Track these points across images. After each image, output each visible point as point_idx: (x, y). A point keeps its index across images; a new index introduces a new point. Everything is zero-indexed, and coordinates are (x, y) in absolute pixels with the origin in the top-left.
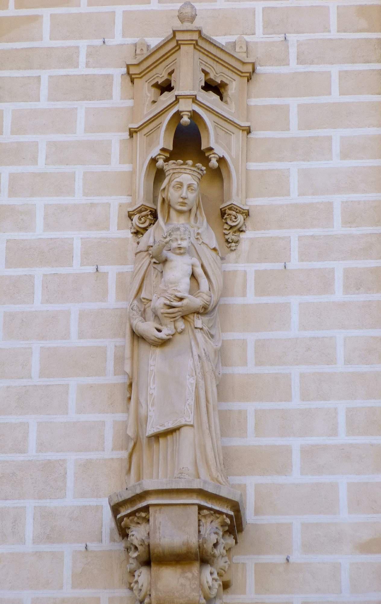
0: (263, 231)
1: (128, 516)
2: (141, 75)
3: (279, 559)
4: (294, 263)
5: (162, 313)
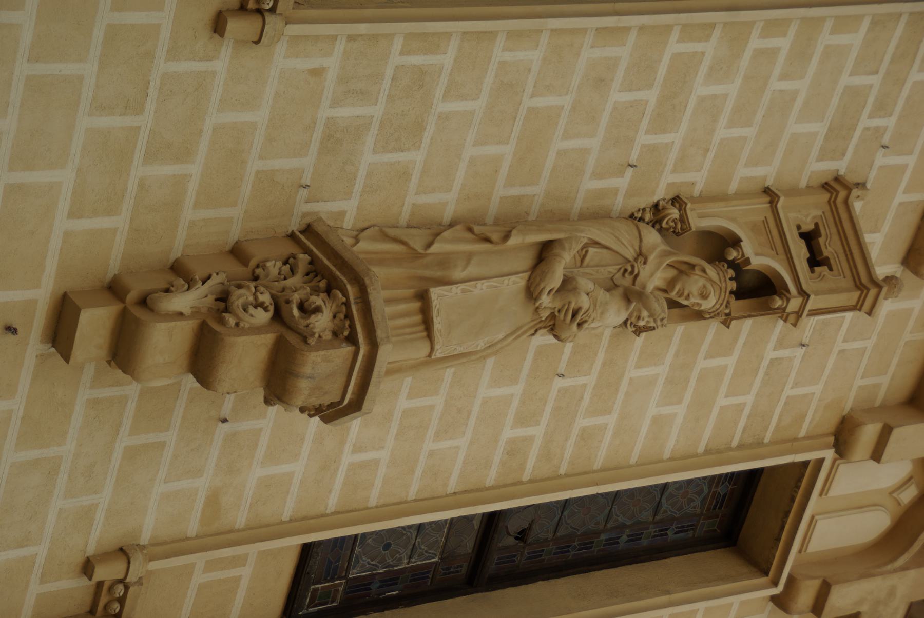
0: (606, 345)
1: (347, 304)
2: (832, 203)
4: (559, 383)
5: (570, 303)
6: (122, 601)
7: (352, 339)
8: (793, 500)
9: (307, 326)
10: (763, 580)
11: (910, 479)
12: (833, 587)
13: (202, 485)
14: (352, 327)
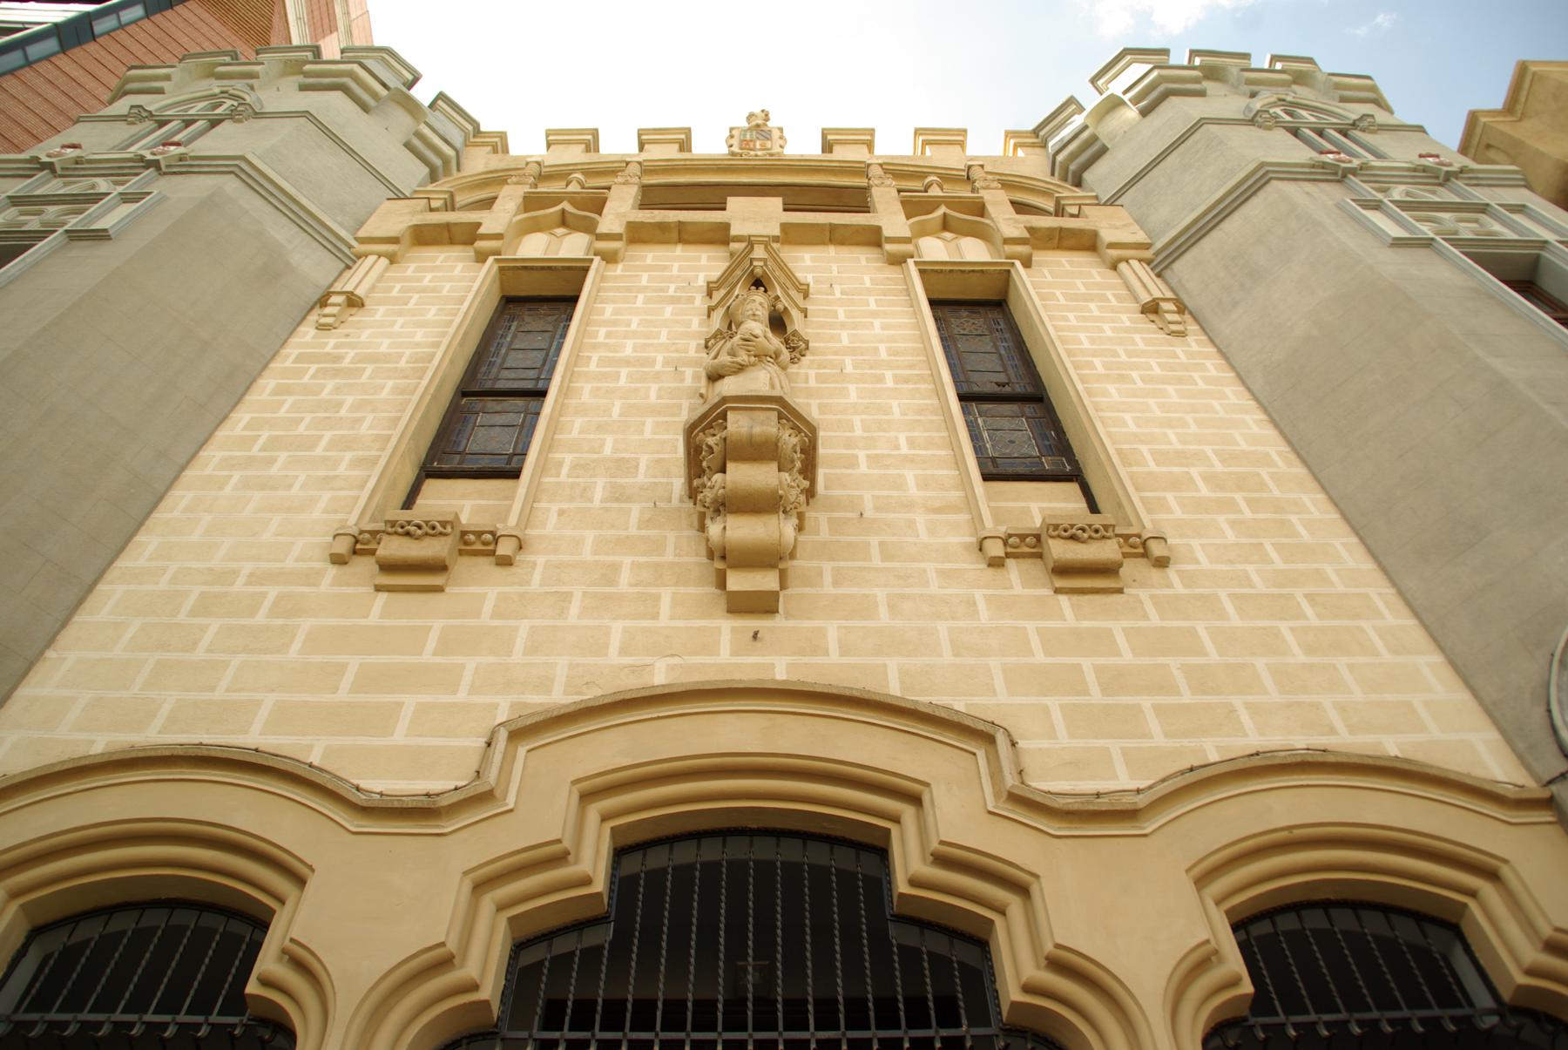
3: (855, 515)
5: (738, 345)
6: (1023, 537)
8: (951, 271)
9: (716, 444)
10: (1013, 272)
11: (938, 238)
12: (1006, 236)
13: (921, 520)
14: (715, 420)
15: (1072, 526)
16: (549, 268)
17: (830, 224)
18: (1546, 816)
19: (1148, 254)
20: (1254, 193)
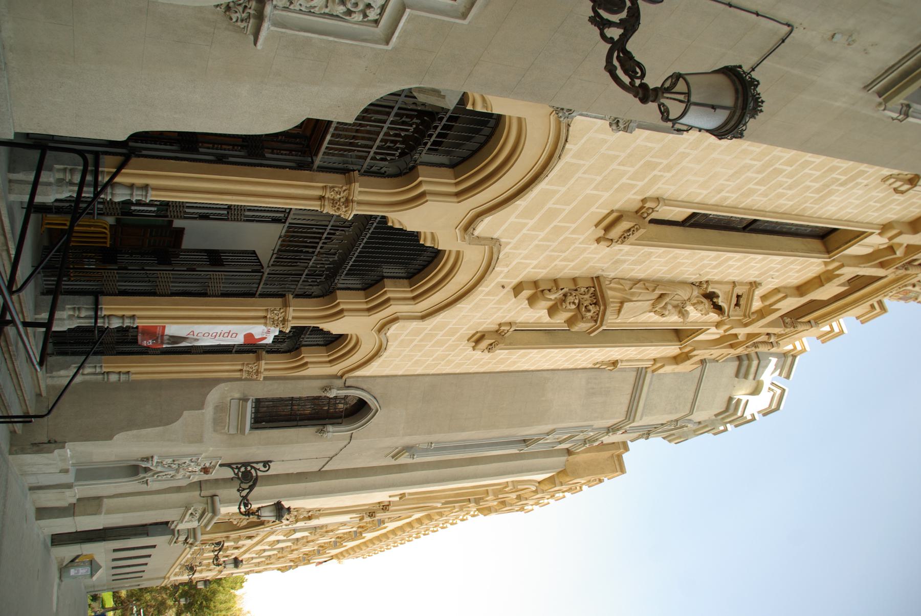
1: (599, 311)
2: (750, 289)
7: (596, 321)
14: (598, 318)
15: (633, 234)
16: (847, 243)
17: (765, 318)
18: (339, 374)
19: (649, 370)
20: (627, 411)
